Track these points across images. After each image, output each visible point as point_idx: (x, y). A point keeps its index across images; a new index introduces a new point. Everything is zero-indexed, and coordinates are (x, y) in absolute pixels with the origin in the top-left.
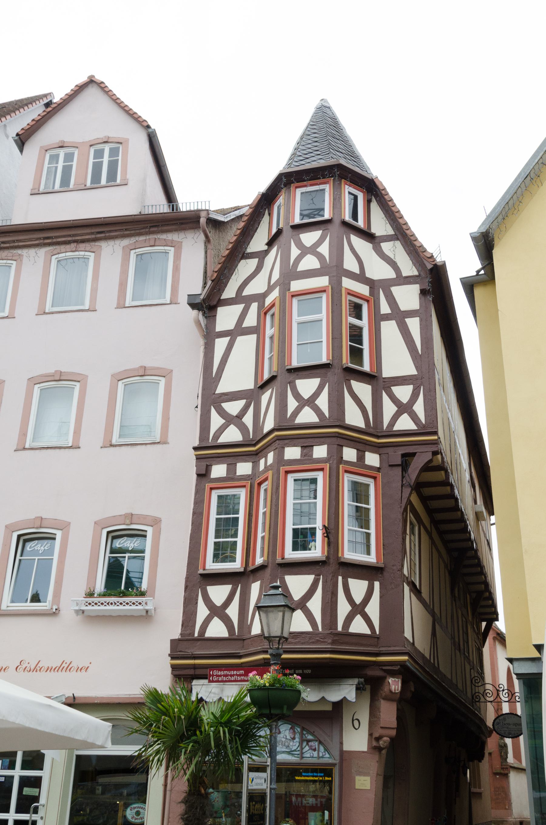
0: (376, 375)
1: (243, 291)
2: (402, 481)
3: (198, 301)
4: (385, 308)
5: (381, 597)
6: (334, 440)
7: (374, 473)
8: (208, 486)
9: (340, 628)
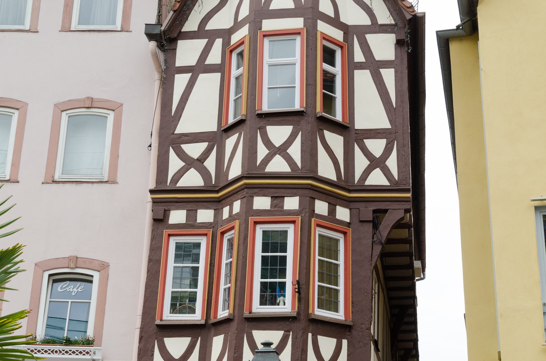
1: (206, 24)
2: (373, 238)
3: (157, 31)
4: (359, 57)
5: (348, 355)
6: (307, 191)
7: (344, 228)
8: (166, 232)
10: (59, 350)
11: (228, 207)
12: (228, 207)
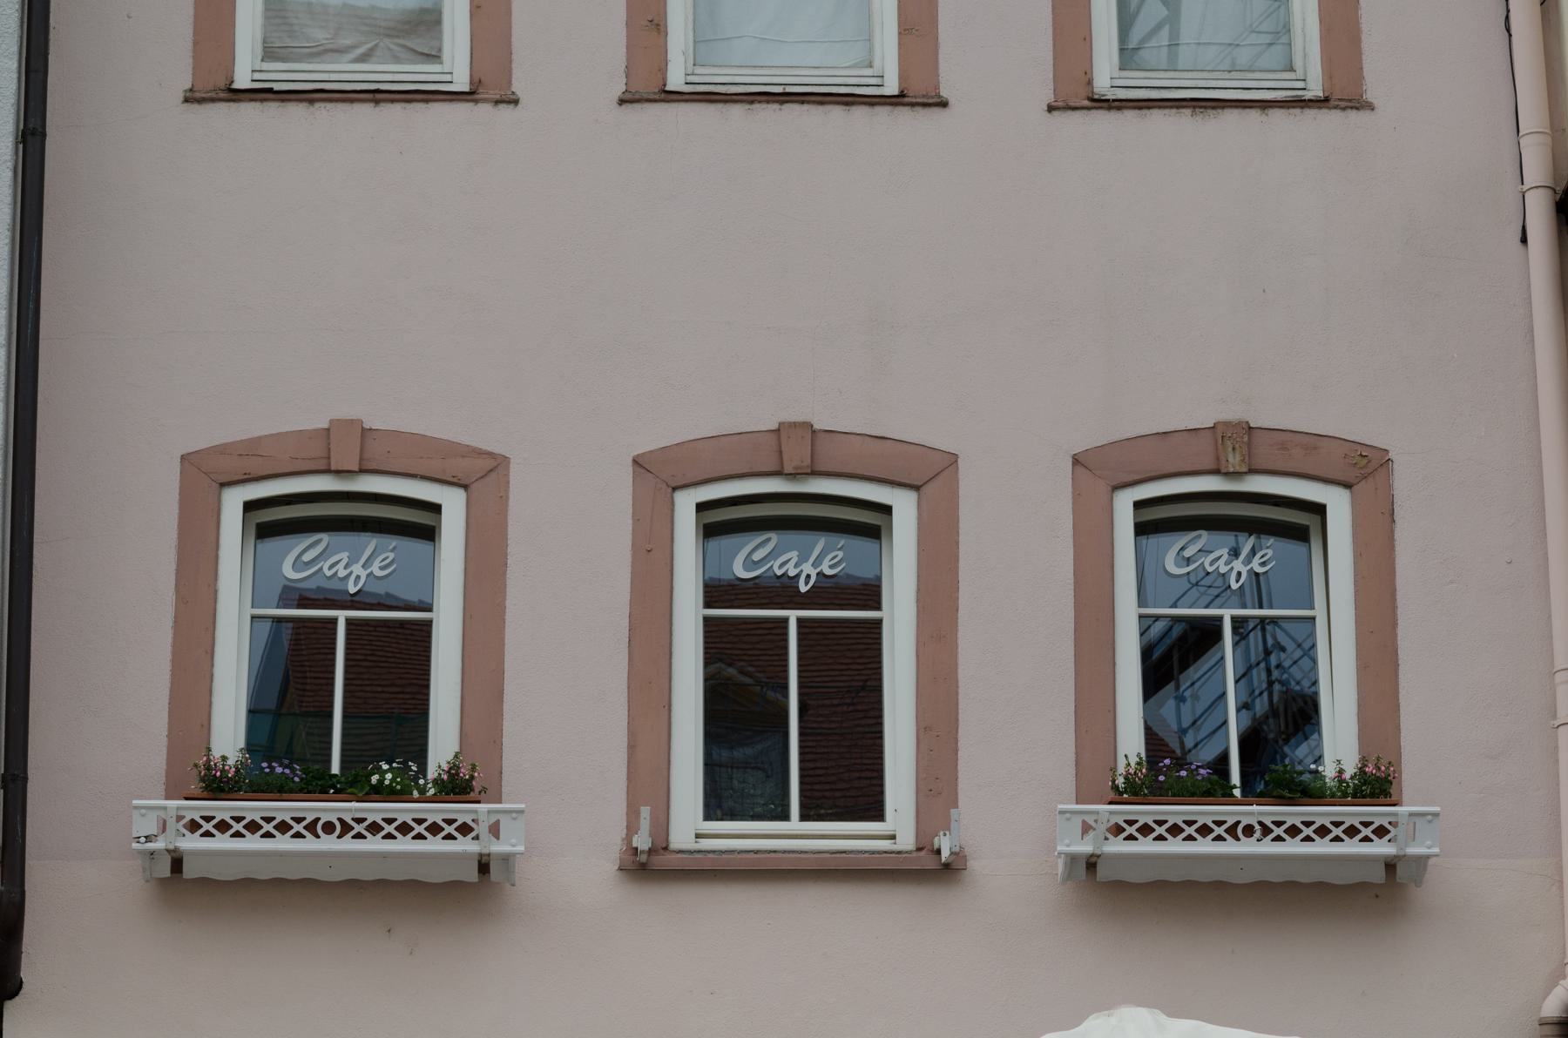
10: (1260, 823)
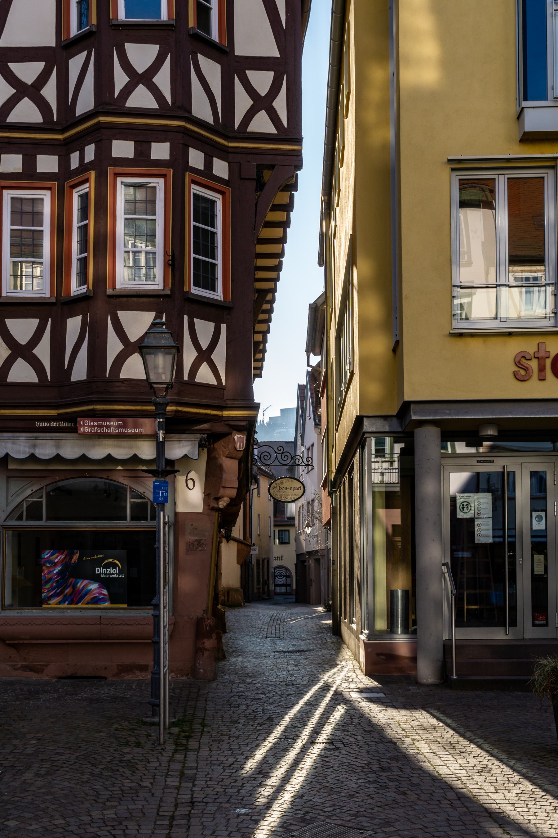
0: (228, 50)
7: (222, 187)
9: (186, 378)
11: (78, 153)
12: (77, 154)
